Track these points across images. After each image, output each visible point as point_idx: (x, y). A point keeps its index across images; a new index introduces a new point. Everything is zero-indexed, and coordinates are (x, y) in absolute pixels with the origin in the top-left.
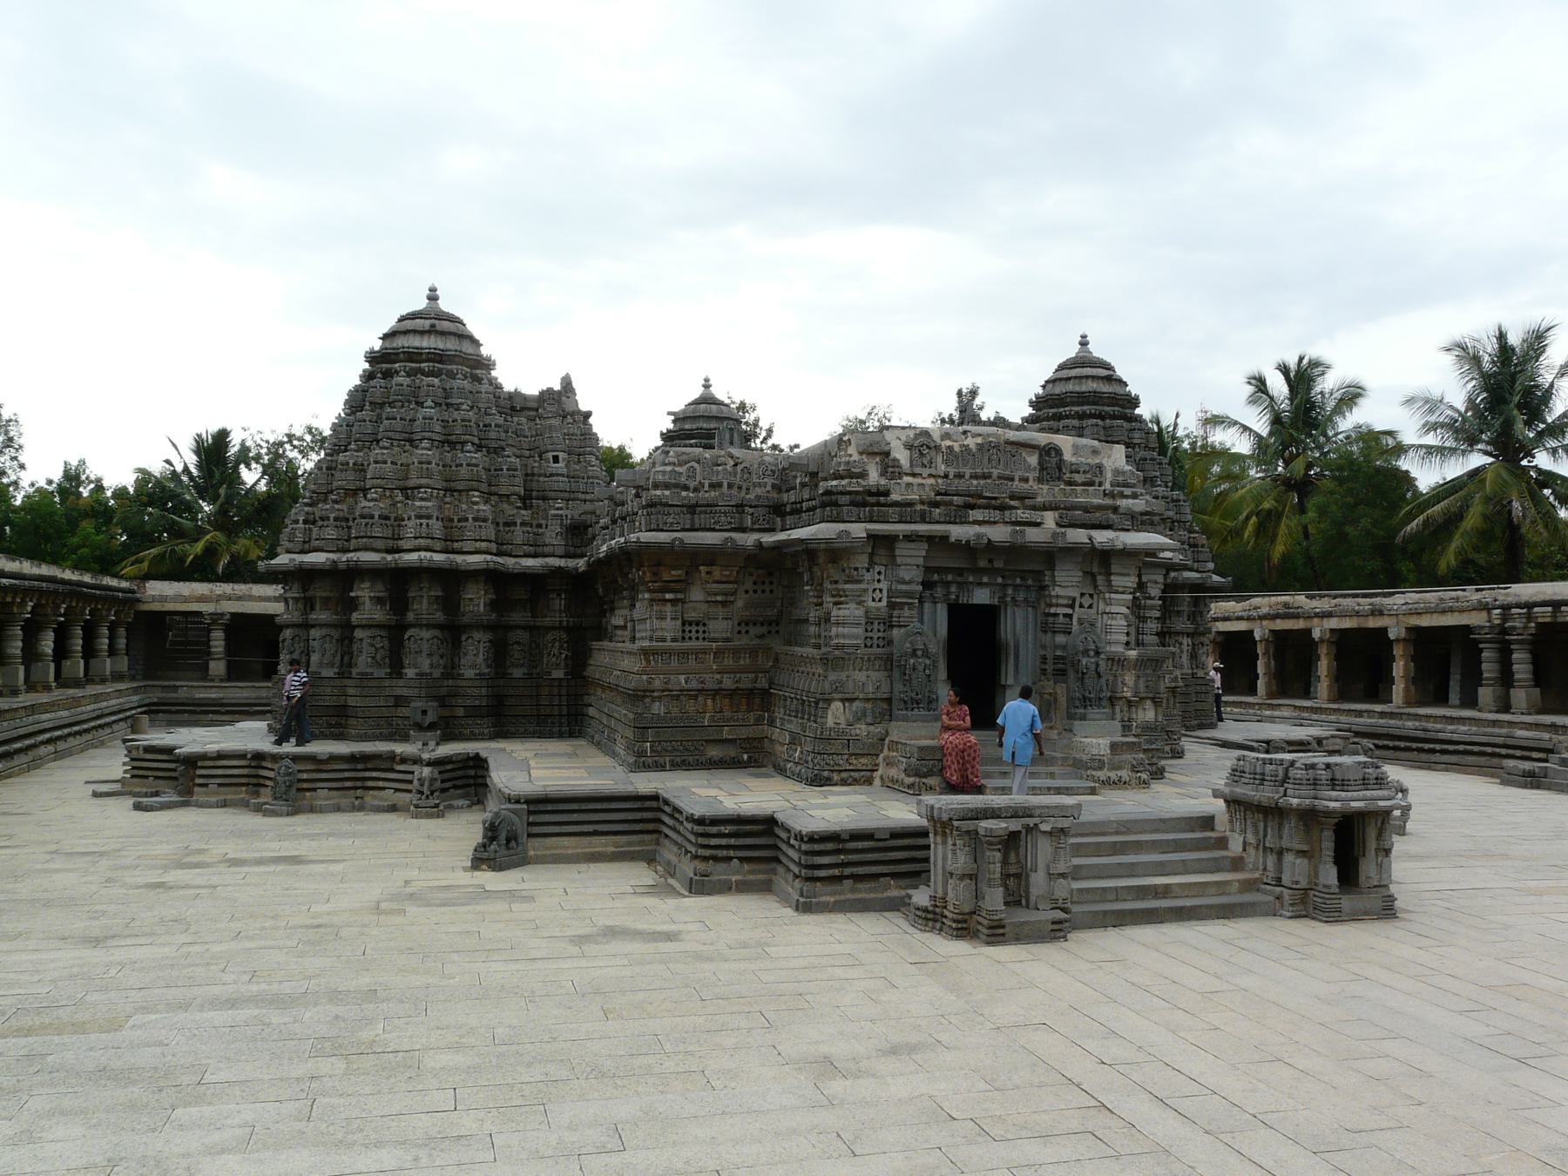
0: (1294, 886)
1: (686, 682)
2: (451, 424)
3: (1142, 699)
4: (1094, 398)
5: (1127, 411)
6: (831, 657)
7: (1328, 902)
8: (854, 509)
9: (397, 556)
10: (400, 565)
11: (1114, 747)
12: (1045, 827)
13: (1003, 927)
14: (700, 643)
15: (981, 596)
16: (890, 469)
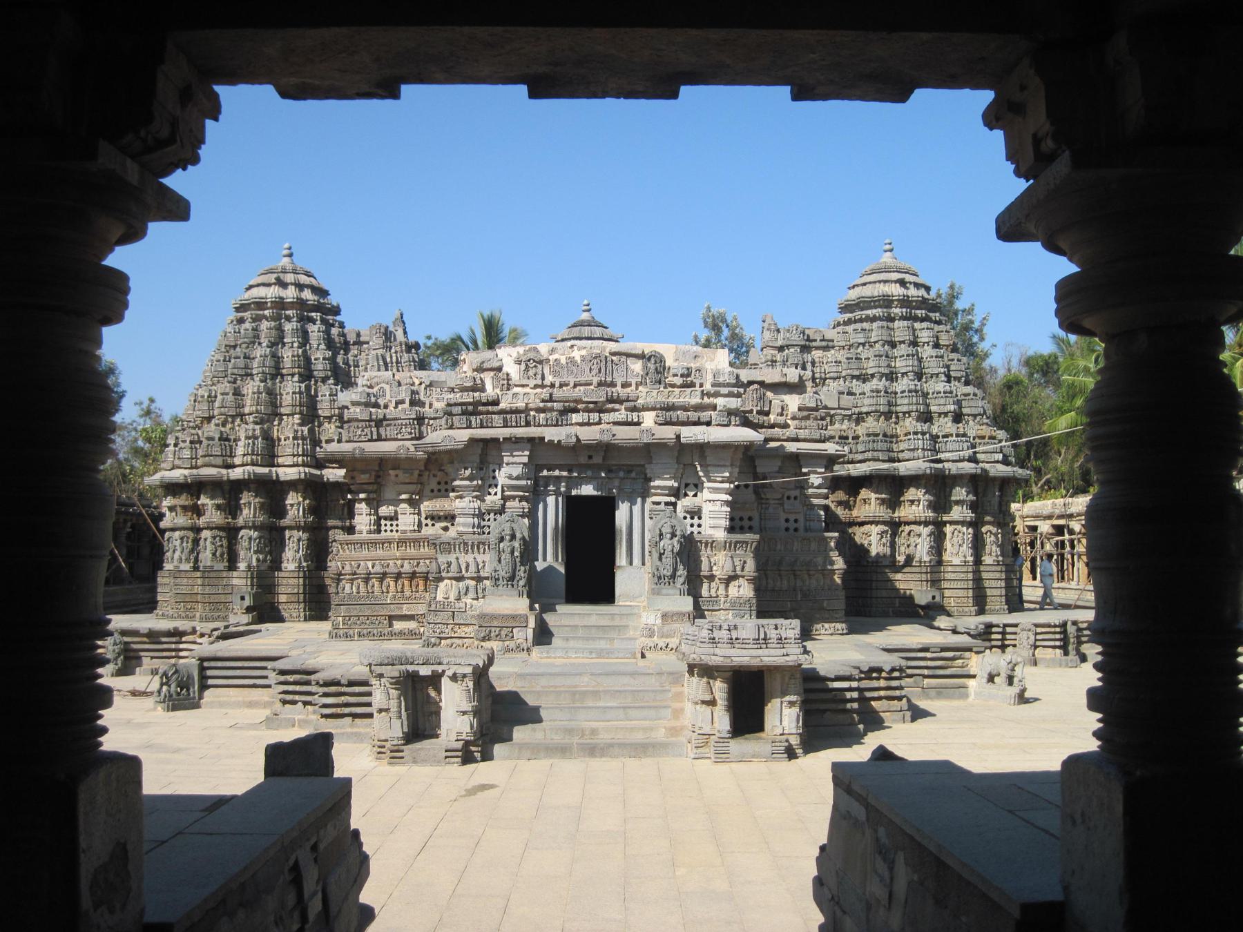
0: (700, 732)
1: (373, 567)
2: (285, 360)
3: (732, 578)
4: (886, 302)
5: (918, 312)
6: (438, 542)
7: (716, 745)
8: (464, 417)
9: (229, 471)
10: (232, 478)
11: (665, 616)
12: (449, 673)
13: (402, 751)
14: (389, 533)
15: (588, 490)
16: (502, 382)
